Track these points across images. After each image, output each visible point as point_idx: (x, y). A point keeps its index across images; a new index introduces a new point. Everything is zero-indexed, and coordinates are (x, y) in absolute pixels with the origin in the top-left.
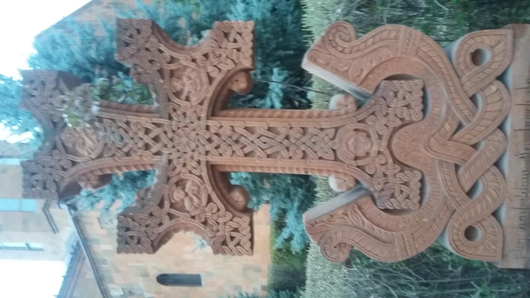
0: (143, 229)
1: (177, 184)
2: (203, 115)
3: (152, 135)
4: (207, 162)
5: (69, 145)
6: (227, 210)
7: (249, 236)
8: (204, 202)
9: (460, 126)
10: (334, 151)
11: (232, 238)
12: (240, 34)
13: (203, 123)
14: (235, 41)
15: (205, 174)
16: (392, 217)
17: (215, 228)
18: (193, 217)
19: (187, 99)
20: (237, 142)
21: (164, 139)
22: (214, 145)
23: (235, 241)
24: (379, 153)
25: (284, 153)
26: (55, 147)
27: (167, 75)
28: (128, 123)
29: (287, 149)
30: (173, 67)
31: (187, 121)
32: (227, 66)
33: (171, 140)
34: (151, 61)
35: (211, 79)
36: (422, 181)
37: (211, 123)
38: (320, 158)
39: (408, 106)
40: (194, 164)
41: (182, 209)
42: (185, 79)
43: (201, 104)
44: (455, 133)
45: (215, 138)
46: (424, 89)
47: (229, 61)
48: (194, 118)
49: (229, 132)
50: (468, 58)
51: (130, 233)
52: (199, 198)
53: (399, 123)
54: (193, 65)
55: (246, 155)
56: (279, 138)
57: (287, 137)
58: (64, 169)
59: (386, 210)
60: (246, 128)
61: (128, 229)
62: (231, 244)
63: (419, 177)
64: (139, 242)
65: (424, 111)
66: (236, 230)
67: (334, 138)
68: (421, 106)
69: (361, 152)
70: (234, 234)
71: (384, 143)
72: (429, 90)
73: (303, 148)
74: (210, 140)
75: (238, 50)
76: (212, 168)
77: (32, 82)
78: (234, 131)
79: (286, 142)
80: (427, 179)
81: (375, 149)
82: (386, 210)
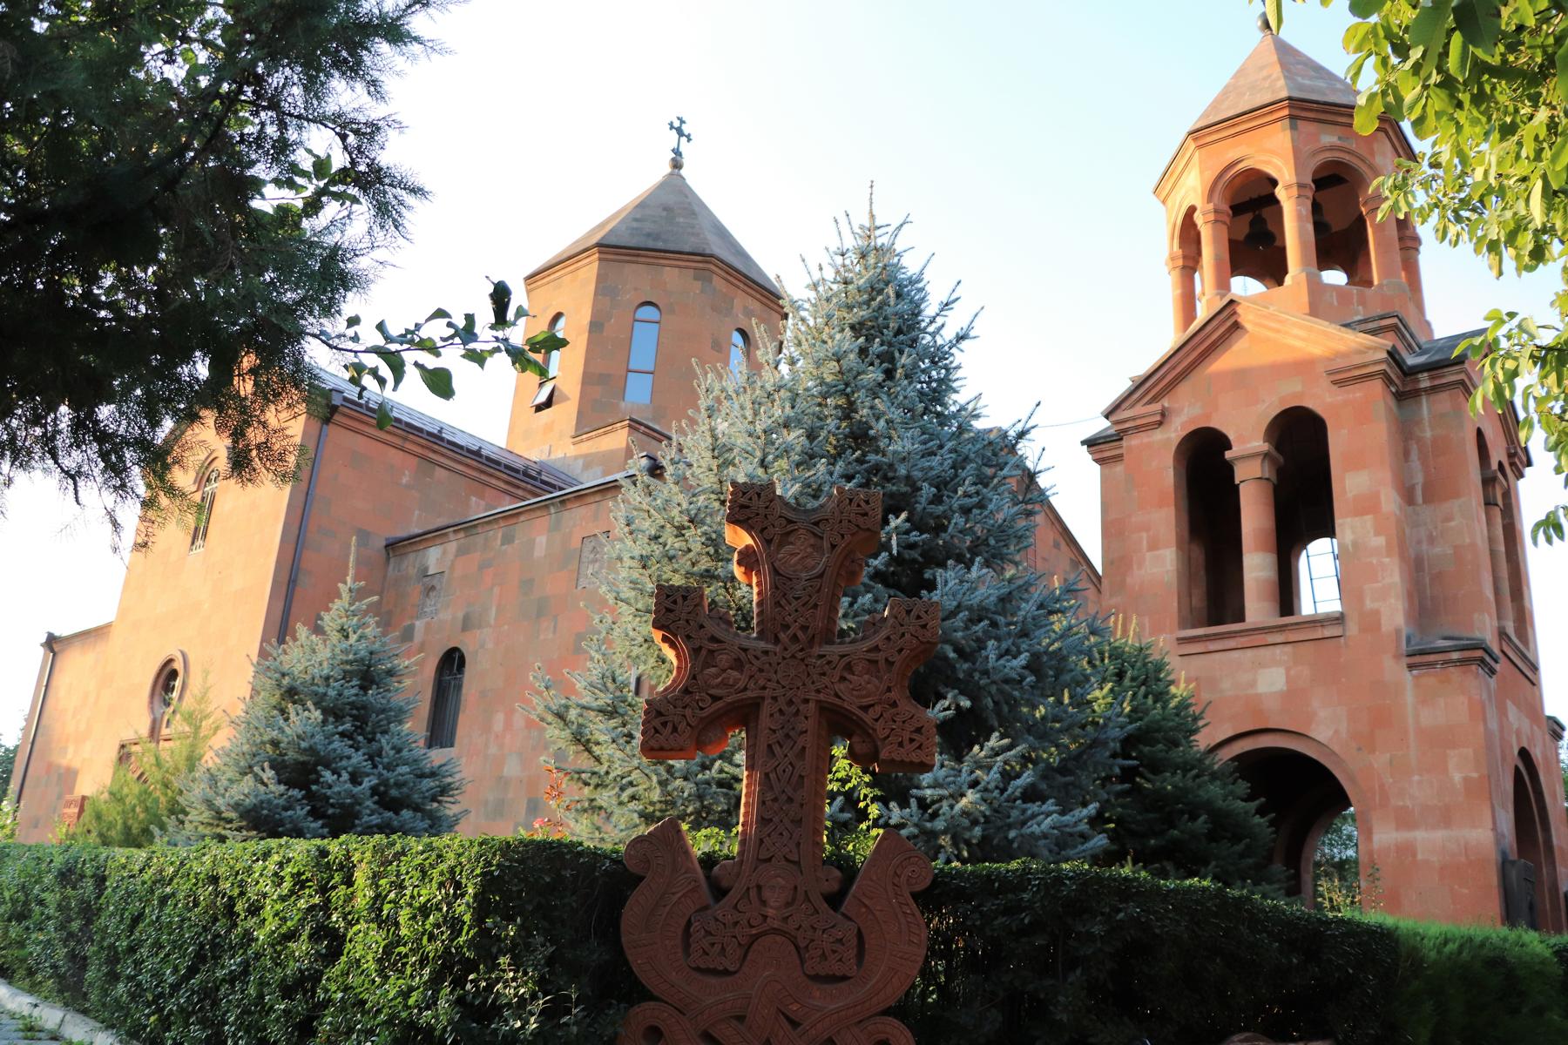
0: (684, 616)
1: (738, 660)
2: (821, 697)
3: (800, 634)
4: (763, 698)
5: (791, 539)
6: (702, 719)
7: (666, 746)
8: (712, 692)
9: (794, 1024)
10: (769, 860)
11: (664, 724)
12: (919, 747)
13: (812, 696)
14: (912, 740)
15: (749, 694)
16: (680, 932)
17: (679, 703)
18: (694, 678)
19: (843, 679)
20: (787, 736)
21: (794, 648)
22: (784, 708)
23: (659, 727)
24: (765, 917)
25: (769, 796)
26: (790, 522)
27: (871, 656)
28: (816, 606)
29: (775, 800)
30: (882, 663)
31: (815, 677)
32: (881, 729)
33: (793, 656)
34: (888, 638)
35: (865, 708)
36: (726, 973)
37: (812, 705)
38: (762, 841)
39: (824, 956)
40: (761, 682)
41: (706, 665)
42: (866, 677)
43: (837, 695)
44: (787, 1018)
45: (793, 709)
46: (844, 978)
47: (887, 732)
48: (818, 685)
49: (800, 727)
50: (883, 1036)
51: (680, 601)
52: (717, 686)
53: (802, 945)
54: (883, 687)
55: (769, 746)
56: (789, 790)
57: (790, 800)
58: (763, 530)
59: (689, 924)
60: (804, 748)
61: (685, 598)
62: (657, 723)
63: (731, 969)
64: (669, 610)
65: (816, 978)
66: (675, 729)
67: (787, 860)
68: (823, 973)
69: (766, 894)
70: (670, 726)
71: (776, 924)
72: (842, 985)
73: (776, 819)
74: (790, 703)
75: (901, 744)
76: (756, 704)
77: (867, 502)
78: (803, 732)
79: (784, 797)
80: (728, 979)
81: (770, 912)
82: (689, 924)
